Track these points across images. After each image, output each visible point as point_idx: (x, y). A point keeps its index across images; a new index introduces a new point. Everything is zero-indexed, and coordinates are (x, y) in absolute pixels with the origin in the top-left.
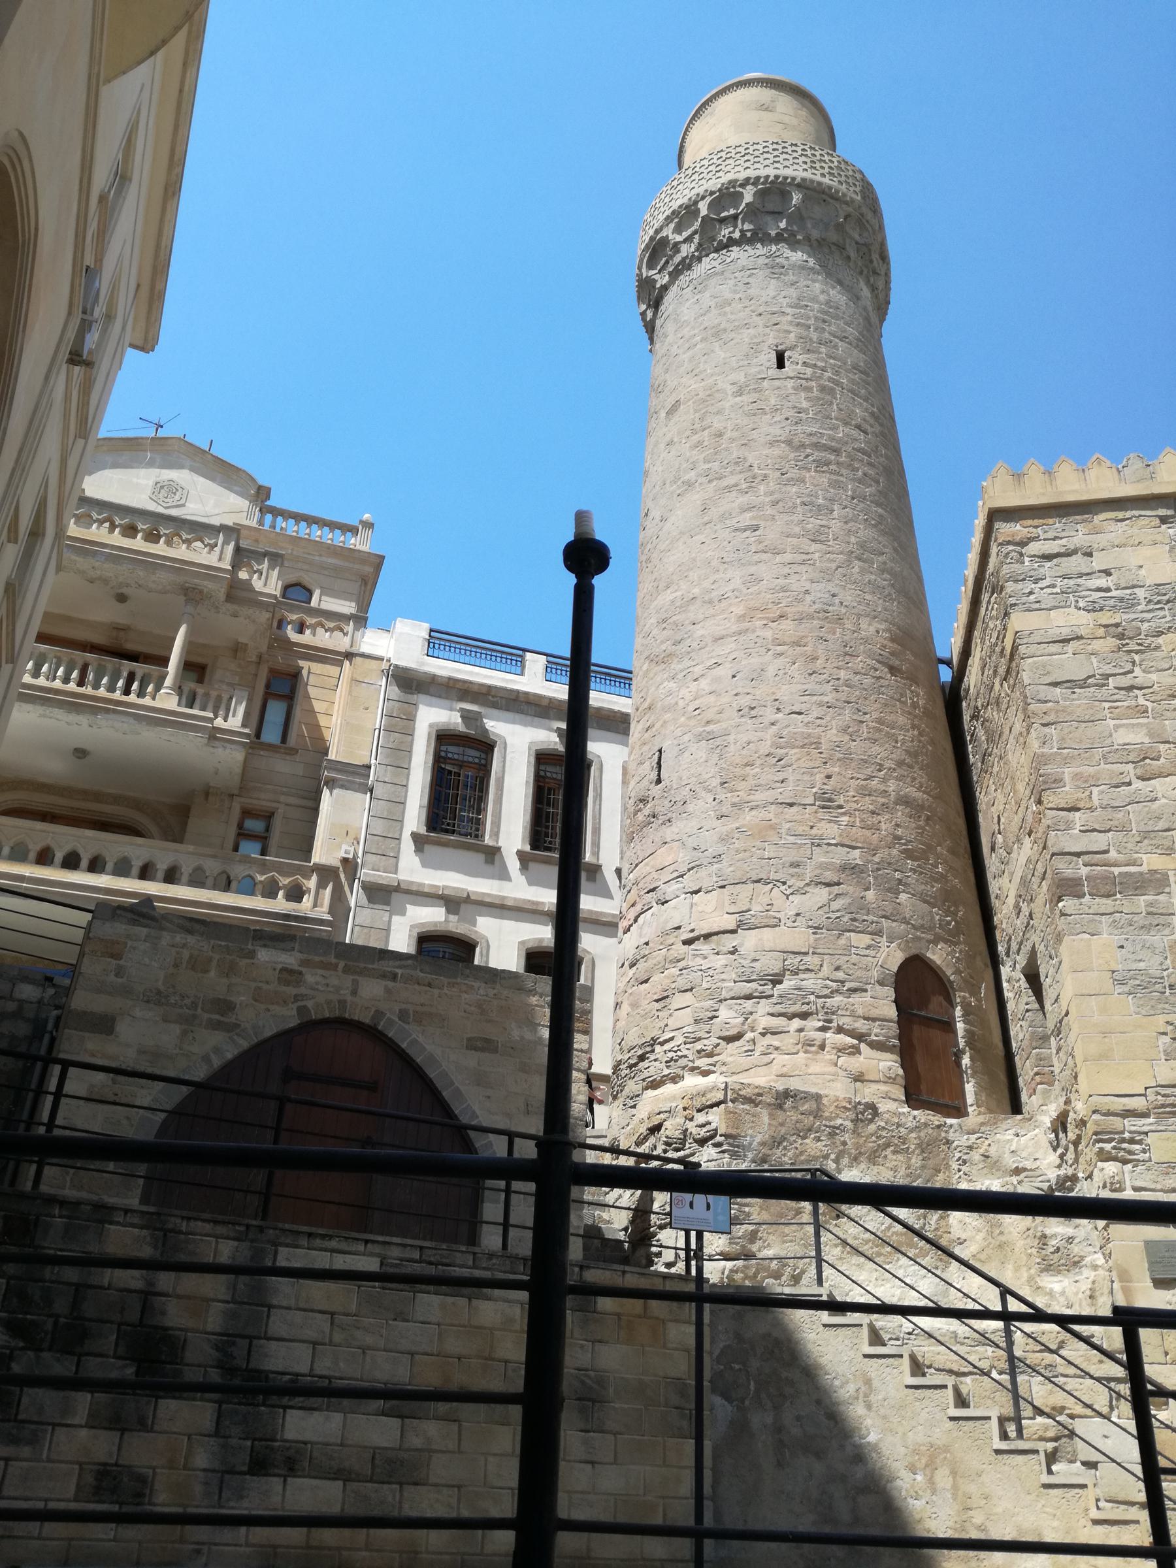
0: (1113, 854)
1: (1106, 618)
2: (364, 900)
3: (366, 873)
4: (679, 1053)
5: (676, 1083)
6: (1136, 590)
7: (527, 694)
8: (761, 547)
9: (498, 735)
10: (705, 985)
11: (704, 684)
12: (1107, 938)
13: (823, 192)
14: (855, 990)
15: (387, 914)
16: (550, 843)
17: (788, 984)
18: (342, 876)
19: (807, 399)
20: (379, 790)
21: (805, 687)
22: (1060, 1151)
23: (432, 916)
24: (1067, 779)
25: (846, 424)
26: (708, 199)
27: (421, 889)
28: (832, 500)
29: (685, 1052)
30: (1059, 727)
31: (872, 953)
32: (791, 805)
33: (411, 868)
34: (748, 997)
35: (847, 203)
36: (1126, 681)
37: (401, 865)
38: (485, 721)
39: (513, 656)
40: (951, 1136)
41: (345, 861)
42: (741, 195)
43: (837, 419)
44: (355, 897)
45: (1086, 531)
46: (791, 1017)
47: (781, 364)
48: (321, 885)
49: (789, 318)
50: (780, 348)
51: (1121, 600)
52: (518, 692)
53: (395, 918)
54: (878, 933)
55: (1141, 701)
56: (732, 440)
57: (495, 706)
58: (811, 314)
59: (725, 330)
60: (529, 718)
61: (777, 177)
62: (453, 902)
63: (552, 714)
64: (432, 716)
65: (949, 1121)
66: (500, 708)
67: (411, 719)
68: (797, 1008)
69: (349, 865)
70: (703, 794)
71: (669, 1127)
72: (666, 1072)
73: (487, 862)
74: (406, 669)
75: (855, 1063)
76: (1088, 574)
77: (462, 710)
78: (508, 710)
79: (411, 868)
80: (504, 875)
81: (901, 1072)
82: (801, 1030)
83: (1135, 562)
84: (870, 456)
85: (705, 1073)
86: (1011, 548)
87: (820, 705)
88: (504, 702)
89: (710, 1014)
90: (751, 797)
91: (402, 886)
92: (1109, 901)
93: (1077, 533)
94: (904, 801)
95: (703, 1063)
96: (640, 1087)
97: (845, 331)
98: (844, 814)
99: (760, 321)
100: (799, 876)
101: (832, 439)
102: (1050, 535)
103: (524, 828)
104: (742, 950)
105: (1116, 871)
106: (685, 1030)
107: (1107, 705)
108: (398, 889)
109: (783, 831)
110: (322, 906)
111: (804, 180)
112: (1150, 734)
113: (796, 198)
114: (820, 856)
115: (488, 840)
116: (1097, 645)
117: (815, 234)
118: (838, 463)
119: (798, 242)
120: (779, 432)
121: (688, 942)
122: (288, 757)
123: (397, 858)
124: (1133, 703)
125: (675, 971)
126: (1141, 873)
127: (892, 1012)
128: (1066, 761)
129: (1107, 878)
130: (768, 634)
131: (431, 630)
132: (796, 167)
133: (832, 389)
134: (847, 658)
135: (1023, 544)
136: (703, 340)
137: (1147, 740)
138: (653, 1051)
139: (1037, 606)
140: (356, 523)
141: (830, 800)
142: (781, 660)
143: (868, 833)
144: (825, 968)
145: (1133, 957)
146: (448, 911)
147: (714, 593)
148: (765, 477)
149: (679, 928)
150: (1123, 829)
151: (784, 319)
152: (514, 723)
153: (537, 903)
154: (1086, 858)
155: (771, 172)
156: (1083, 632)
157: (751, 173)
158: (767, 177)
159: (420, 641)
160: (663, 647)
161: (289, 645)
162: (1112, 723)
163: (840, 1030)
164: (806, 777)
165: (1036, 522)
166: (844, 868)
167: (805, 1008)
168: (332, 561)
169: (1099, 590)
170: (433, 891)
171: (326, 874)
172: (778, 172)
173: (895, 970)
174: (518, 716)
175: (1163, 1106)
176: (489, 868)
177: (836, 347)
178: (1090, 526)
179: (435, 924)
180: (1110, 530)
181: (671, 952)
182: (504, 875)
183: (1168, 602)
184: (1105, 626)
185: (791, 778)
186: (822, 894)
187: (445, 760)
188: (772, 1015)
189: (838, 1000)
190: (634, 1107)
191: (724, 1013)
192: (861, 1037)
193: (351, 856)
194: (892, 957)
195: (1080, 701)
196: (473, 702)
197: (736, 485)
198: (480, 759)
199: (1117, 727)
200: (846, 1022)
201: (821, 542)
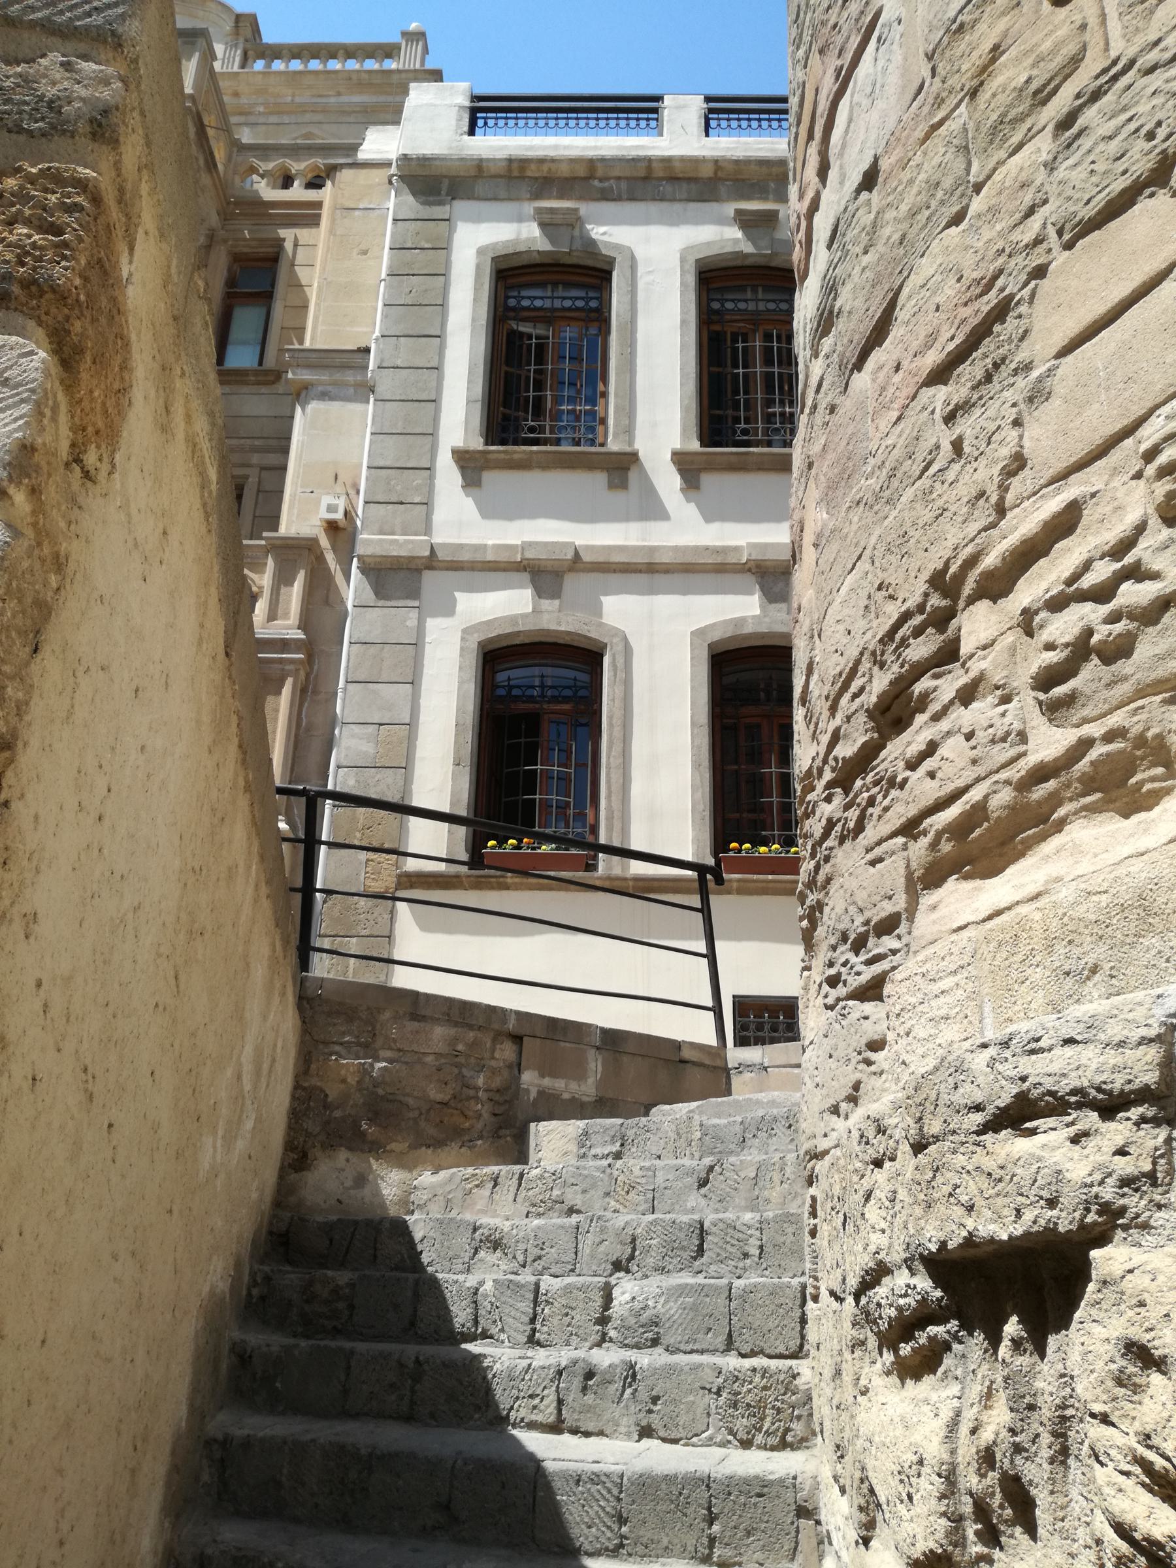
2: (369, 595)
3: (370, 542)
4: (1132, 594)
7: (667, 161)
9: (618, 247)
15: (414, 614)
16: (745, 432)
18: (330, 557)
20: (387, 384)
23: (507, 606)
27: (479, 557)
33: (458, 519)
37: (439, 516)
38: (589, 227)
39: (642, 108)
41: (332, 527)
44: (353, 588)
48: (283, 579)
52: (649, 160)
53: (435, 626)
57: (605, 196)
60: (677, 207)
62: (545, 574)
63: (723, 190)
64: (483, 235)
66: (618, 199)
67: (444, 247)
69: (340, 531)
72: (1049, 742)
73: (612, 486)
74: (424, 160)
77: (539, 211)
78: (632, 199)
79: (458, 519)
80: (653, 510)
88: (624, 185)
91: (441, 555)
96: (893, 872)
103: (685, 409)
106: (1151, 433)
108: (432, 561)
110: (286, 615)
115: (614, 445)
122: (264, 390)
123: (427, 504)
131: (476, 98)
138: (949, 654)
140: (396, 38)
146: (540, 593)
152: (647, 222)
153: (724, 550)
159: (454, 112)
161: (257, 208)
168: (357, 99)
170: (503, 557)
171: (297, 554)
174: (654, 208)
176: (619, 497)
179: (513, 619)
182: (653, 510)
187: (518, 313)
190: (872, 991)
193: (339, 516)
196: (561, 196)
198: (587, 299)
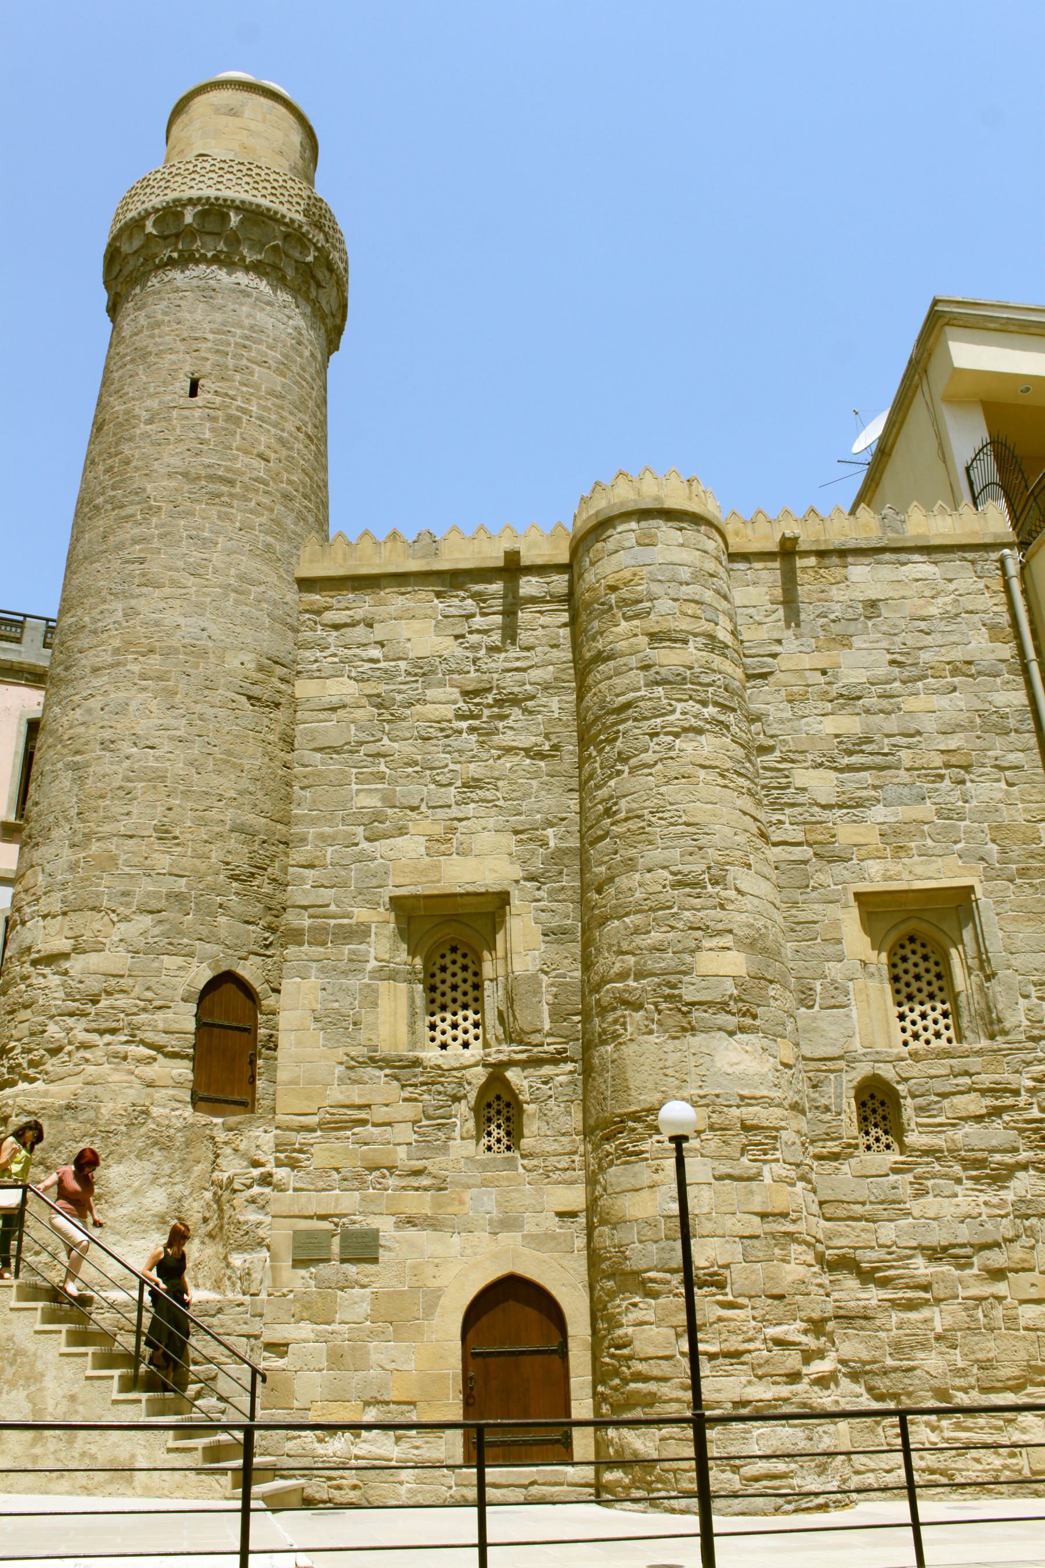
1: (370, 688)
6: (400, 663)
8: (143, 580)
10: (41, 1002)
12: (314, 981)
13: (262, 214)
14: (160, 1008)
19: (212, 430)
21: (161, 722)
24: (310, 838)
25: (246, 452)
26: (152, 218)
28: (217, 533)
30: (313, 790)
31: (182, 973)
32: (131, 837)
34: (71, 1015)
35: (286, 225)
36: (373, 748)
40: (215, 1133)
42: (182, 214)
43: (238, 449)
45: (372, 602)
46: (102, 1032)
47: (193, 393)
49: (210, 345)
50: (196, 375)
51: (386, 671)
54: (191, 955)
55: (383, 768)
56: (137, 469)
58: (232, 340)
59: (150, 353)
61: (217, 199)
65: (216, 1120)
68: (105, 1025)
70: (63, 822)
75: (149, 1072)
76: (365, 645)
81: (191, 1077)
82: (109, 1044)
83: (407, 634)
84: (267, 484)
86: (307, 616)
87: (171, 738)
89: (40, 1028)
90: (100, 829)
92: (321, 949)
93: (364, 605)
94: (238, 828)
95: (31, 1072)
97: (266, 355)
98: (178, 844)
99: (181, 347)
100: (128, 905)
101: (228, 469)
102: (342, 605)
104: (72, 973)
105: (332, 922)
107: (355, 771)
109: (120, 862)
111: (243, 202)
112: (384, 799)
113: (234, 219)
114: (147, 886)
116: (359, 714)
117: (250, 257)
118: (231, 495)
119: (234, 264)
120: (179, 463)
121: (34, 963)
124: (374, 769)
125: (23, 987)
126: (350, 925)
127: (191, 1025)
128: (314, 822)
130: (136, 668)
132: (238, 188)
133: (239, 418)
134: (206, 692)
135: (318, 613)
136: (133, 361)
137: (379, 804)
139: (317, 674)
141: (167, 832)
142: (144, 695)
143: (197, 862)
144: (137, 988)
145: (331, 998)
147: (100, 624)
148: (160, 508)
150: (344, 885)
151: (204, 346)
154: (311, 910)
155: (212, 193)
156: (348, 700)
157: (194, 194)
158: (209, 198)
162: (354, 787)
163: (142, 1042)
164: (148, 810)
165: (332, 593)
166: (168, 896)
167: (114, 1025)
169: (372, 660)
172: (219, 193)
173: (201, 986)
175: (329, 1123)
177: (252, 374)
178: (376, 597)
180: (396, 601)
183: (424, 674)
184: (368, 696)
185: (135, 811)
186: (148, 920)
188: (87, 1031)
189: (144, 1017)
191: (52, 1029)
192: (159, 1048)
194: (203, 975)
195: (333, 766)
197: (132, 516)
199: (358, 791)
200: (150, 1036)
201: (200, 576)
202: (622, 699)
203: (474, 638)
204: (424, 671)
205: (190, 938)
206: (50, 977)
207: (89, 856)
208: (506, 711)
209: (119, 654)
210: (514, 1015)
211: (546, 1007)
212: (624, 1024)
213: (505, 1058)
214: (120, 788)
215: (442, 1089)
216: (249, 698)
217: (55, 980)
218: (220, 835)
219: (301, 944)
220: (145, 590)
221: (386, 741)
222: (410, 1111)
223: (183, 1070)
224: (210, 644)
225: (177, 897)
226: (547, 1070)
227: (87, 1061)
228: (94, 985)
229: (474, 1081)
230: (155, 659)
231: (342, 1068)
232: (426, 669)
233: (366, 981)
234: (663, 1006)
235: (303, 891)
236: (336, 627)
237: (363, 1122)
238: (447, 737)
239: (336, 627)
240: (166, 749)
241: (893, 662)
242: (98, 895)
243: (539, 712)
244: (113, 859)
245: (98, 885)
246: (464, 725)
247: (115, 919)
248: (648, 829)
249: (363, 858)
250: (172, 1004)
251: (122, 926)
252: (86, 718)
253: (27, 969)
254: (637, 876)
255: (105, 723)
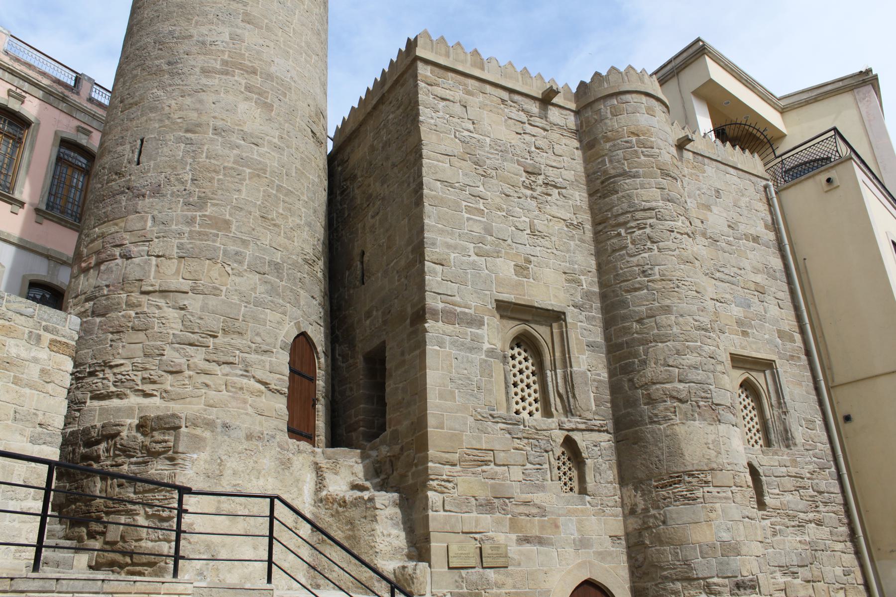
0: (457, 299)
5: (121, 399)
11: (188, 101)
17: (221, 340)
22: (383, 476)
24: (438, 243)
29: (133, 377)
34: (191, 345)
36: (475, 191)
71: (125, 438)
72: (113, 389)
85: (147, 395)
95: (148, 388)
100: (240, 263)
104: (190, 308)
105: (459, 309)
107: (464, 203)
127: (287, 371)
128: (441, 232)
129: (451, 312)
149: (141, 280)
160: (157, 62)
162: (467, 215)
167: (231, 359)
181: (131, 298)
195: (451, 195)
199: (468, 219)
200: (259, 374)
202: (648, 205)
203: (527, 137)
204: (503, 150)
205: (283, 300)
206: (166, 309)
207: (205, 216)
208: (550, 192)
209: (227, 66)
210: (574, 396)
211: (592, 395)
212: (675, 412)
213: (574, 427)
214: (232, 168)
215: (537, 443)
216: (312, 132)
217: (172, 314)
218: (299, 226)
219: (437, 321)
220: (248, 26)
221: (481, 188)
222: (519, 457)
223: (280, 405)
224: (293, 84)
225: (277, 267)
226: (595, 436)
227: (207, 385)
228: (214, 323)
229: (558, 440)
230: (257, 81)
231: (472, 419)
232: (503, 148)
233: (483, 357)
234: (701, 403)
235: (437, 282)
236: (443, 99)
237: (486, 463)
238: (519, 198)
239: (443, 99)
240: (266, 149)
241: (729, 226)
242: (215, 249)
243: (569, 199)
244: (227, 223)
245: (214, 241)
246: (529, 192)
247: (230, 272)
248: (676, 289)
249: (474, 266)
250: (274, 350)
251: (238, 280)
252: (198, 106)
253: (136, 297)
254: (673, 318)
255: (216, 114)
